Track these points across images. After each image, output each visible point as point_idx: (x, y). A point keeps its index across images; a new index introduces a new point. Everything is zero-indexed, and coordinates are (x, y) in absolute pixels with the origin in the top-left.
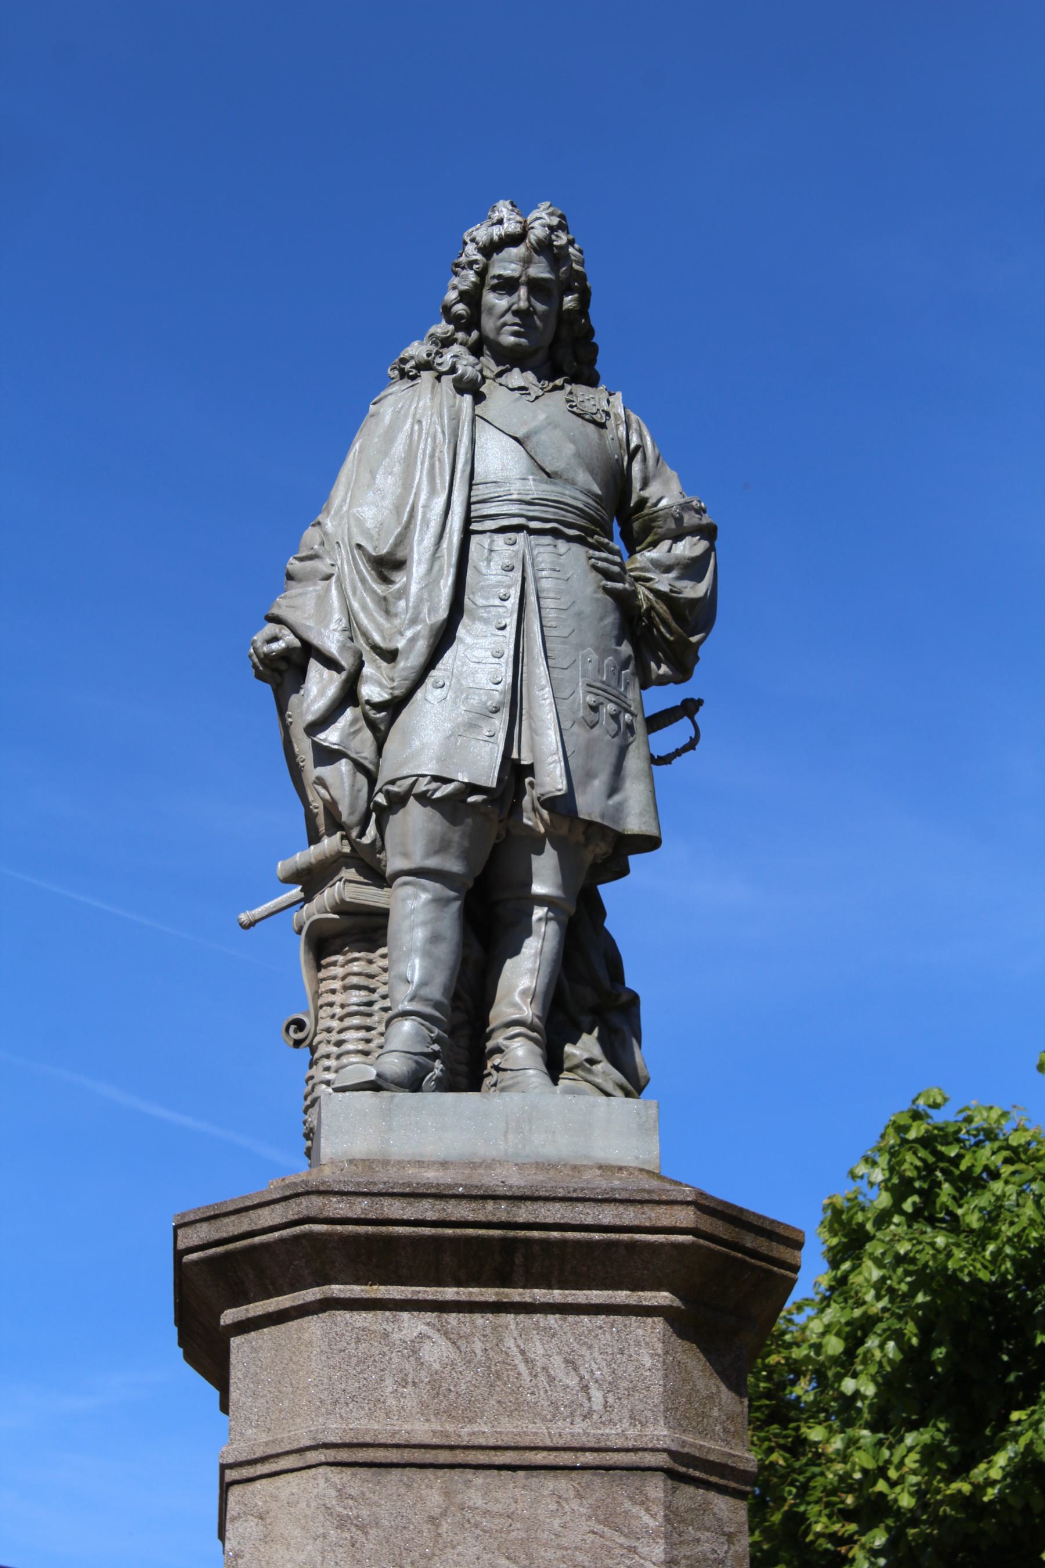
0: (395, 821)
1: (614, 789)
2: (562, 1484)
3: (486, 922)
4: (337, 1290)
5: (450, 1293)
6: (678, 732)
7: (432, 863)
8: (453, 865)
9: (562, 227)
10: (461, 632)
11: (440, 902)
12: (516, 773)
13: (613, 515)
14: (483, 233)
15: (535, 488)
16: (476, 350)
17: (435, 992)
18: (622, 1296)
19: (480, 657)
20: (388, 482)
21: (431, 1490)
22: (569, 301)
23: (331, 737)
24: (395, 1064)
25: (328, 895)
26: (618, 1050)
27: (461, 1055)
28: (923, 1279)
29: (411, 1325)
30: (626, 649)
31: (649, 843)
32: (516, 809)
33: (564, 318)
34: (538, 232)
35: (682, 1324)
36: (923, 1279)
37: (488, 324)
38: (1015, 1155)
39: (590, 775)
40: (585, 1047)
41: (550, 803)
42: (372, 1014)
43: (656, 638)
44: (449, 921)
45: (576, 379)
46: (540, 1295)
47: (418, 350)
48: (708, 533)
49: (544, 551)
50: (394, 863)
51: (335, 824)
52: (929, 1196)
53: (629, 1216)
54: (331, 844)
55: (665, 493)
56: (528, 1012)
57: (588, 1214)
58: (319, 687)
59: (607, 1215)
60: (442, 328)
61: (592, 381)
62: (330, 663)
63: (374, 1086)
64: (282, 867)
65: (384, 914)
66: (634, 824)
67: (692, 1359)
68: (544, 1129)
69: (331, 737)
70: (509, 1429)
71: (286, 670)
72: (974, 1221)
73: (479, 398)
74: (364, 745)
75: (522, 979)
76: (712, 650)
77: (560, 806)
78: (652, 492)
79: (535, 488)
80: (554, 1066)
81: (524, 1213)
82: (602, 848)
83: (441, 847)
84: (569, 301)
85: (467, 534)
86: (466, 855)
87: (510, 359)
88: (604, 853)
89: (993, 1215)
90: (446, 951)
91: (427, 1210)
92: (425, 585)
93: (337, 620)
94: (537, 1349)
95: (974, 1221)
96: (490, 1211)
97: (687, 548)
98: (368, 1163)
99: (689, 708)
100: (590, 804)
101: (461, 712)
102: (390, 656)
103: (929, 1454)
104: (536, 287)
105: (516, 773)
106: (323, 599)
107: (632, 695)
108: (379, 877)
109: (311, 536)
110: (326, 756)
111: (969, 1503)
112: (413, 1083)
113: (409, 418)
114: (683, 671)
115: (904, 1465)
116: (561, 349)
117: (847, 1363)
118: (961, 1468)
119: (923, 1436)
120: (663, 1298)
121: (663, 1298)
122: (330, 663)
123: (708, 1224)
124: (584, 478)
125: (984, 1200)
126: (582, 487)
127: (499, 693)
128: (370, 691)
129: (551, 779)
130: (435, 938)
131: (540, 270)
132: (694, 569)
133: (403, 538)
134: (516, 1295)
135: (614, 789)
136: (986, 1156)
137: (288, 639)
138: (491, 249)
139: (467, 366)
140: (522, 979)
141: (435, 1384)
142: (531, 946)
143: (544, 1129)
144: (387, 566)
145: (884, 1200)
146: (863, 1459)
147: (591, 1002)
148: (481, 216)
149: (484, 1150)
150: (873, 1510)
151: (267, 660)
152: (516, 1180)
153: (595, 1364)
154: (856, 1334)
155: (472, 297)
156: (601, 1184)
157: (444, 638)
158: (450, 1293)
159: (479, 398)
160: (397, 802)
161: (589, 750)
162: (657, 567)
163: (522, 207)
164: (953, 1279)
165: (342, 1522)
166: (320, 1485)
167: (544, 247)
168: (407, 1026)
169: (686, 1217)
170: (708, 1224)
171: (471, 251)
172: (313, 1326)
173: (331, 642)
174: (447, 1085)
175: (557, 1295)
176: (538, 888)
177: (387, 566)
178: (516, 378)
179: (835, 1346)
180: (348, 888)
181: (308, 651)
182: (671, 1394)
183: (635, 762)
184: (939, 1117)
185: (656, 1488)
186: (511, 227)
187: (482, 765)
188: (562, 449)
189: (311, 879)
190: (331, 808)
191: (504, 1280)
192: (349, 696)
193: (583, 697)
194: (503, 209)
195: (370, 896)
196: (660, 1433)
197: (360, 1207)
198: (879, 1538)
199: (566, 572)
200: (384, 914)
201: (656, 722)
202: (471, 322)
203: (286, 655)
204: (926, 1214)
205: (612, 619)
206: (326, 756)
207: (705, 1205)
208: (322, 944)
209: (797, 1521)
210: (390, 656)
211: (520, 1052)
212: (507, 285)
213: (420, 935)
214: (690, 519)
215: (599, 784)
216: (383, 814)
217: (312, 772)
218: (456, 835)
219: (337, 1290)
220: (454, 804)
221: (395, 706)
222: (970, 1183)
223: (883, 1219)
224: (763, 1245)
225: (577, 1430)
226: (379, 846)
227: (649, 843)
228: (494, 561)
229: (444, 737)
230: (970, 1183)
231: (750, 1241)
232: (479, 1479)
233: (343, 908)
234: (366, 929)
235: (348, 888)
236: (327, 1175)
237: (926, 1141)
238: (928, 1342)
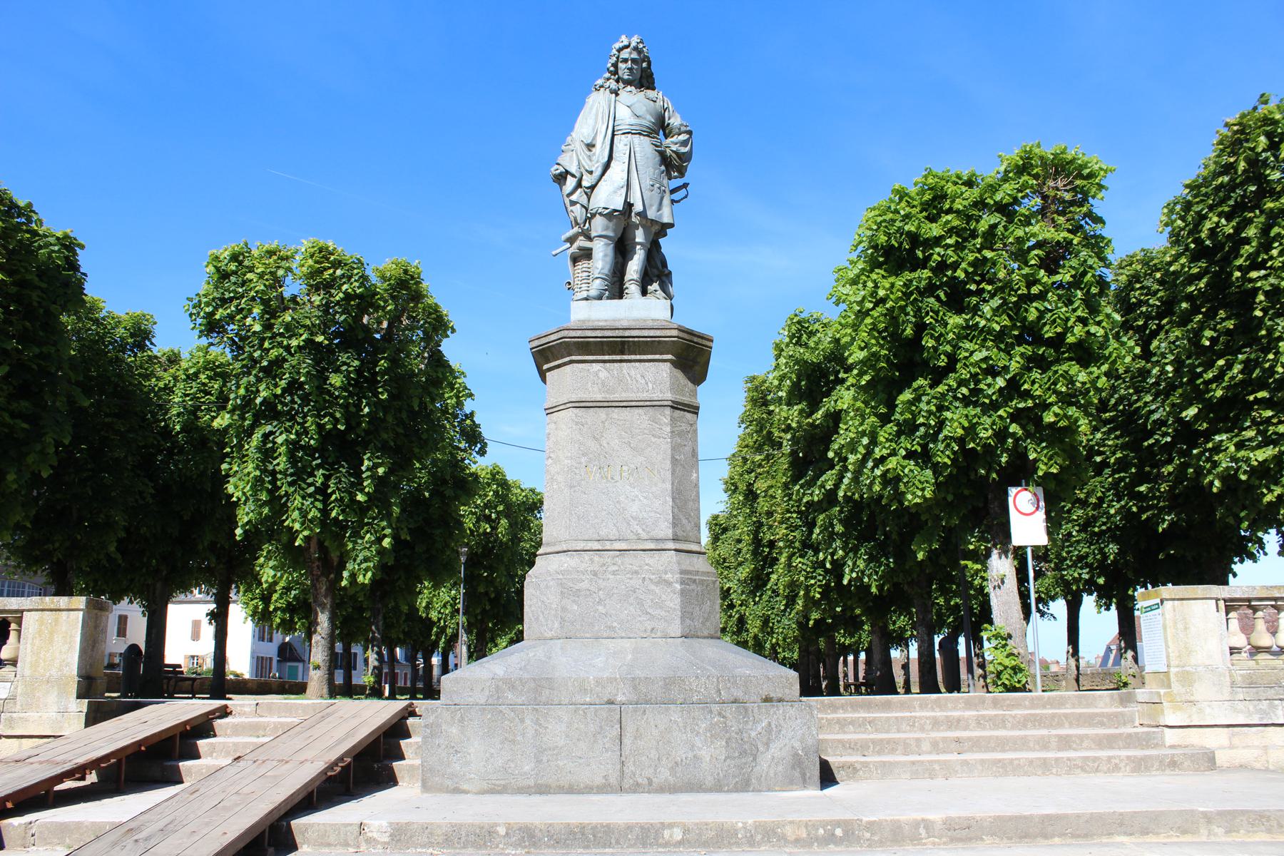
0: (593, 221)
1: (659, 209)
2: (640, 411)
3: (622, 249)
4: (574, 358)
5: (607, 357)
6: (682, 193)
7: (604, 233)
8: (611, 234)
9: (642, 42)
10: (612, 164)
11: (607, 245)
12: (629, 206)
13: (660, 127)
14: (618, 45)
15: (634, 121)
16: (617, 81)
17: (606, 271)
18: (657, 357)
19: (617, 172)
20: (591, 122)
21: (602, 413)
22: (644, 65)
23: (574, 198)
24: (593, 293)
25: (576, 245)
26: (664, 289)
27: (616, 288)
28: (797, 362)
29: (596, 367)
30: (663, 168)
31: (671, 225)
32: (630, 216)
33: (643, 70)
34: (634, 44)
35: (675, 364)
36: (797, 362)
37: (620, 73)
38: (825, 325)
39: (651, 206)
40: (655, 286)
41: (638, 214)
42: (588, 280)
43: (673, 165)
44: (610, 250)
45: (648, 88)
46: (633, 357)
47: (600, 82)
48: (690, 133)
49: (636, 138)
50: (593, 234)
51: (577, 224)
52: (800, 338)
53: (658, 333)
54: (576, 229)
55: (675, 121)
56: (636, 276)
57: (646, 333)
58: (571, 182)
59: (652, 333)
60: (607, 75)
61: (653, 89)
62: (573, 176)
63: (586, 299)
64: (563, 237)
65: (591, 249)
66: (666, 220)
67: (679, 374)
68: (641, 310)
69: (574, 198)
70: (624, 396)
71: (561, 178)
72: (812, 345)
73: (617, 95)
74: (584, 200)
75: (634, 267)
76: (692, 168)
77: (642, 214)
78: (671, 121)
79: (634, 121)
80: (644, 293)
81: (627, 333)
82: (655, 228)
83: (607, 228)
84: (644, 65)
85: (613, 135)
86: (615, 231)
87: (627, 83)
88: (663, 229)
89: (817, 344)
90: (610, 258)
91: (598, 333)
92: (601, 153)
93: (575, 163)
94: (633, 373)
95: (812, 345)
96: (617, 333)
97: (683, 137)
98: (584, 321)
99: (685, 186)
100: (651, 214)
101: (612, 189)
102: (591, 173)
103: (801, 412)
104: (633, 61)
105: (629, 206)
106: (571, 157)
107: (665, 181)
108: (590, 239)
109: (569, 139)
110: (573, 203)
111: (812, 425)
112: (600, 298)
113: (598, 102)
114: (682, 174)
115: (793, 414)
116: (644, 80)
117: (779, 388)
118: (809, 415)
119: (800, 407)
120: (670, 357)
121: (670, 357)
122: (573, 176)
123: (682, 335)
124: (649, 117)
125: (815, 339)
126: (648, 120)
127: (624, 182)
128: (585, 183)
129: (638, 207)
130: (606, 255)
131: (635, 55)
132: (684, 143)
133: (594, 138)
134: (626, 357)
135: (659, 209)
136: (816, 326)
137: (562, 169)
138: (620, 50)
139: (613, 85)
140: (634, 267)
141: (603, 384)
142: (636, 257)
143: (641, 310)
144: (590, 146)
145: (787, 340)
146: (784, 414)
147: (656, 273)
148: (617, 40)
149: (618, 316)
150: (789, 428)
151: (555, 176)
152: (625, 324)
153: (649, 376)
154: (782, 378)
155: (615, 65)
156: (650, 324)
157: (607, 166)
158: (607, 357)
159: (617, 95)
160: (593, 215)
161: (651, 198)
162: (672, 144)
163: (629, 36)
164: (806, 362)
165: (577, 424)
166: (571, 413)
167: (636, 49)
168: (598, 281)
169: (675, 333)
170: (682, 335)
171: (614, 51)
172: (568, 368)
173: (573, 170)
174: (608, 298)
175: (638, 357)
176: (637, 240)
177: (590, 146)
178: (629, 88)
179: (776, 383)
180: (581, 242)
181: (567, 172)
182: (672, 384)
183: (666, 201)
184: (803, 316)
185: (668, 411)
186: (626, 43)
187: (619, 205)
188: (641, 110)
189: (571, 240)
190: (575, 219)
191: (623, 353)
192: (579, 185)
193: (649, 182)
194: (623, 38)
195: (587, 244)
196: (669, 396)
197: (579, 333)
198: (789, 436)
199: (644, 147)
200: (591, 249)
201: (673, 192)
202: (616, 73)
203: (560, 174)
204: (798, 343)
205: (658, 158)
206: (573, 203)
207: (681, 329)
208: (575, 260)
209: (770, 433)
210: (591, 173)
211: (633, 289)
212: (625, 61)
213: (601, 254)
214: (683, 129)
215: (655, 208)
216: (590, 219)
217: (570, 208)
218: (611, 225)
219: (574, 358)
220: (610, 215)
221: (593, 188)
222: (811, 334)
223: (787, 345)
224: (700, 341)
225: (645, 396)
226: (589, 230)
227: (671, 225)
228: (621, 143)
229: (609, 196)
230: (811, 334)
231: (696, 339)
232: (616, 410)
233: (580, 249)
234: (587, 254)
235: (581, 242)
236: (572, 325)
237: (799, 322)
238: (799, 380)
